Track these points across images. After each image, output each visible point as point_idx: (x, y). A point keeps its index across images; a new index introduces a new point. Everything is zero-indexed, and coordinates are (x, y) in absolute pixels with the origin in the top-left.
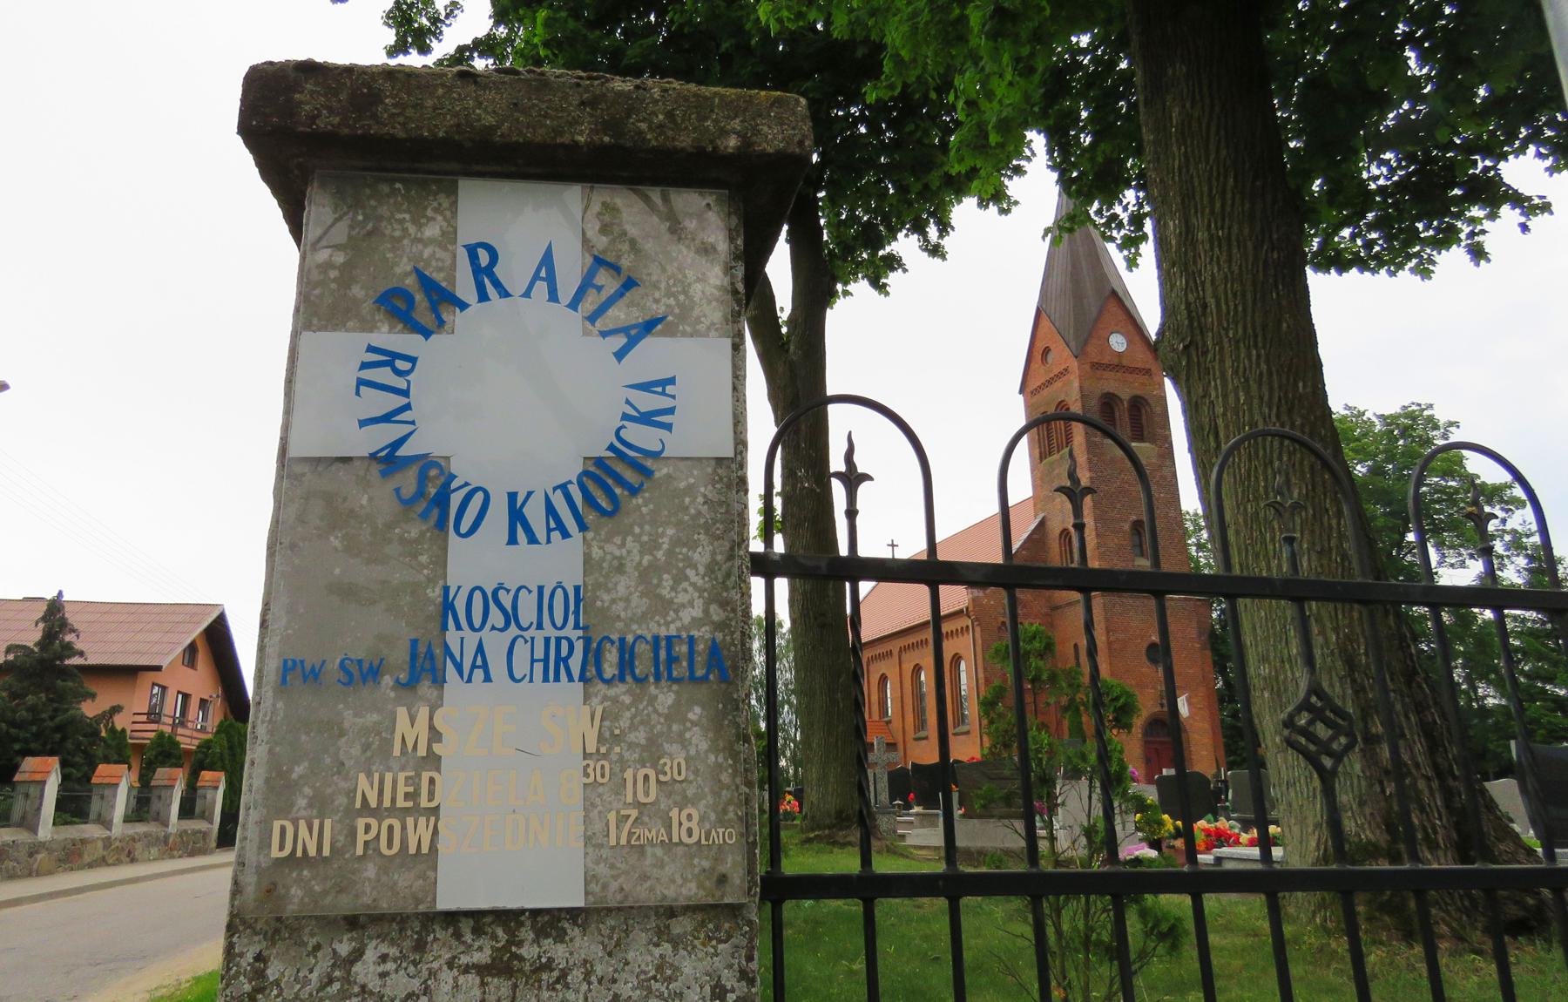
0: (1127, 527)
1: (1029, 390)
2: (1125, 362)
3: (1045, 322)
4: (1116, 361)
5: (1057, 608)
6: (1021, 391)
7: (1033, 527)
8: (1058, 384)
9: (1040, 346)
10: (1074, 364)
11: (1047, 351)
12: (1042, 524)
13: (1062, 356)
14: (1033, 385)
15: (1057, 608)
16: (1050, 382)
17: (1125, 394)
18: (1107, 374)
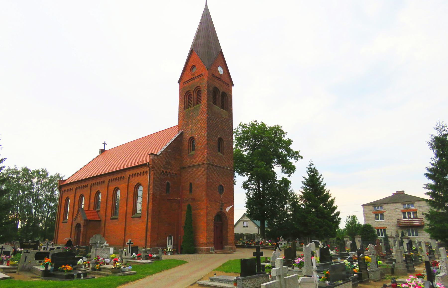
0: (217, 139)
1: (182, 82)
2: (222, 78)
3: (194, 57)
4: (219, 76)
5: (183, 168)
6: (179, 82)
7: (178, 135)
8: (197, 80)
9: (190, 65)
10: (206, 72)
11: (193, 67)
12: (182, 134)
13: (201, 68)
14: (185, 79)
15: (183, 168)
16: (193, 79)
17: (221, 90)
18: (216, 80)
